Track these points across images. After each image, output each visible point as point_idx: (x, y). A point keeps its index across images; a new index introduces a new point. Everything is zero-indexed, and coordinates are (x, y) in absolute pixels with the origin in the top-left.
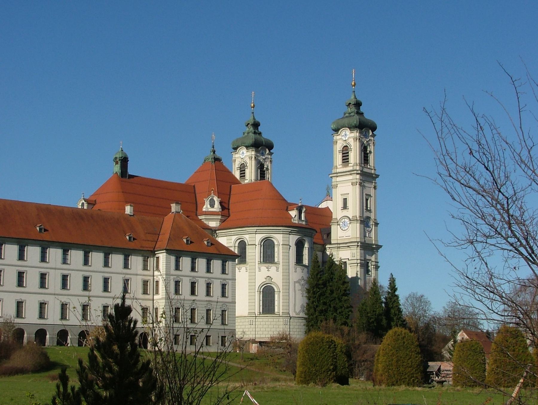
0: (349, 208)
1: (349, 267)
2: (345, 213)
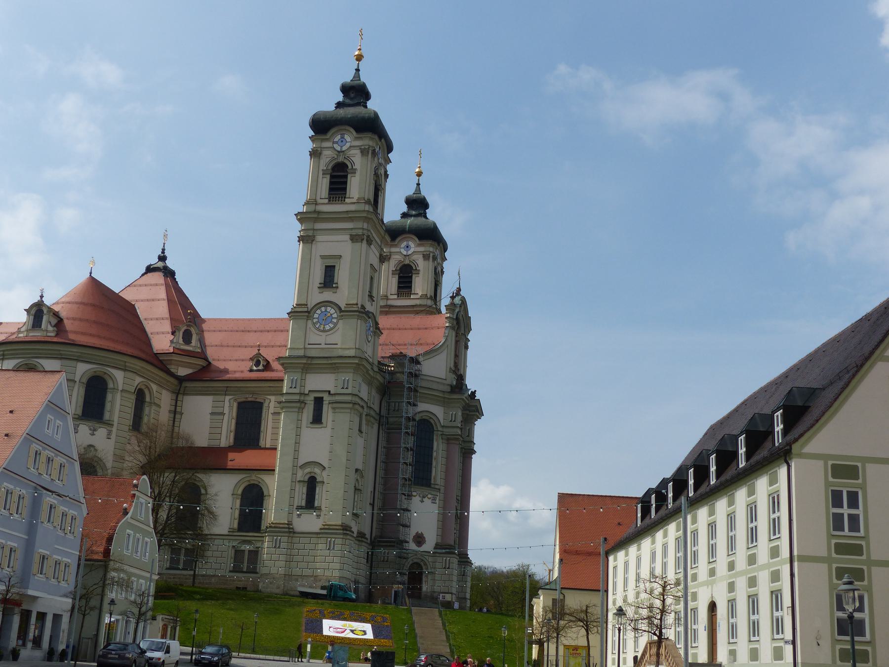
0: (340, 285)
1: (330, 411)
2: (328, 295)
